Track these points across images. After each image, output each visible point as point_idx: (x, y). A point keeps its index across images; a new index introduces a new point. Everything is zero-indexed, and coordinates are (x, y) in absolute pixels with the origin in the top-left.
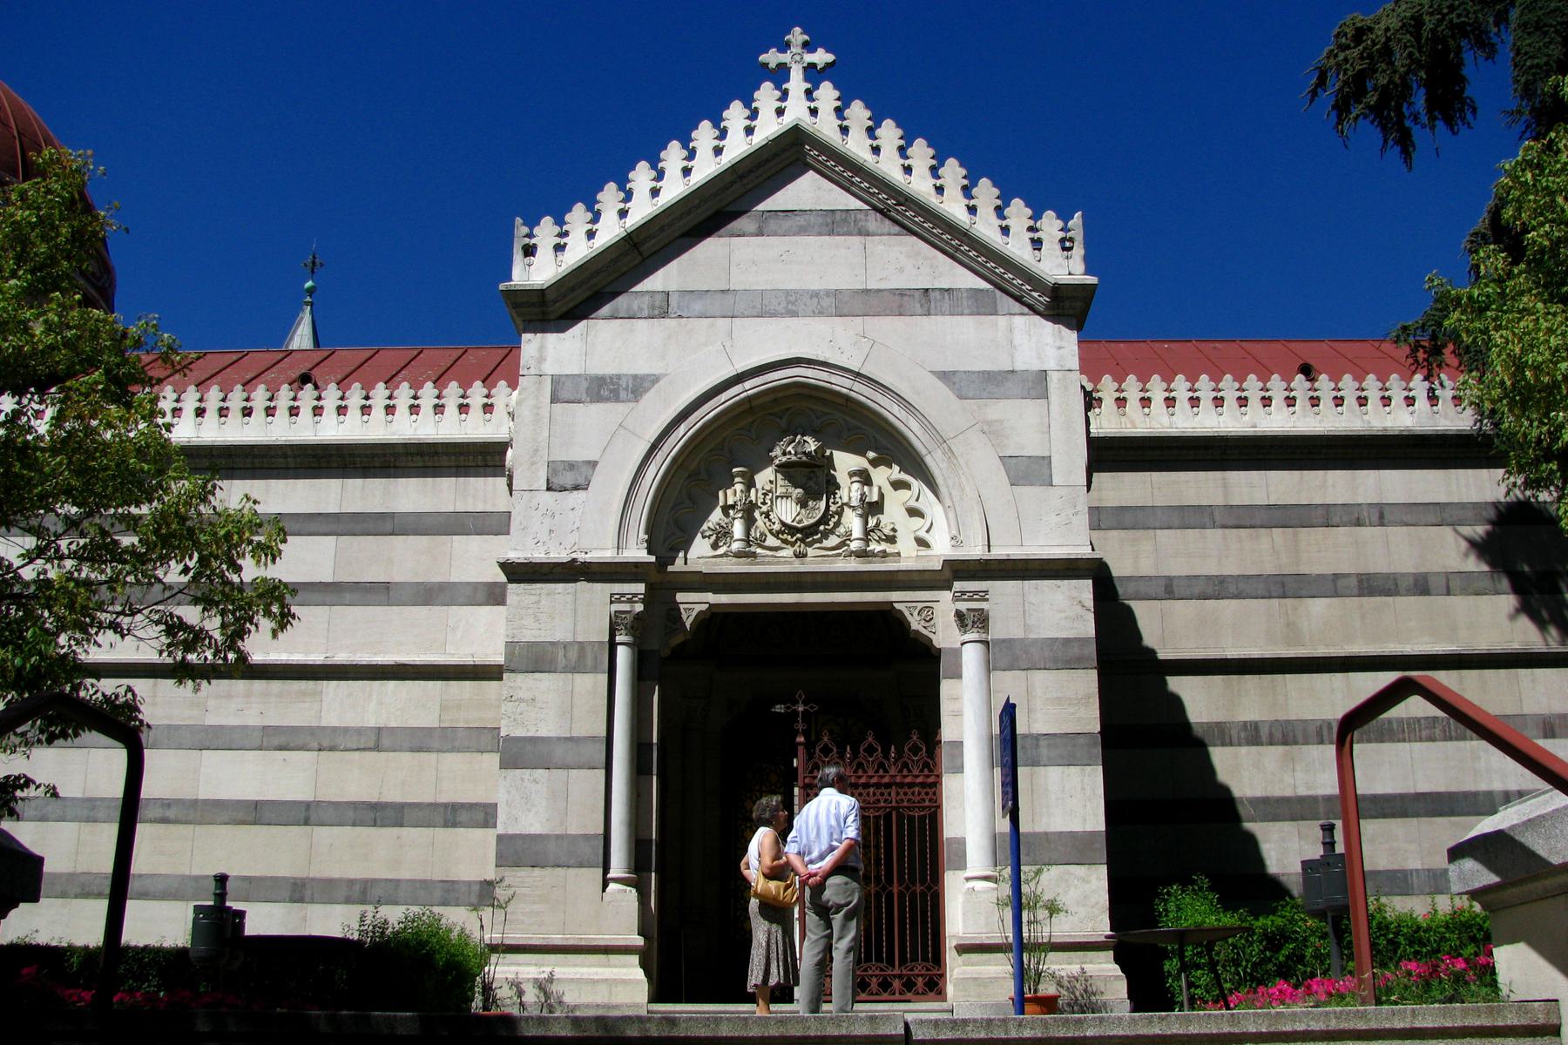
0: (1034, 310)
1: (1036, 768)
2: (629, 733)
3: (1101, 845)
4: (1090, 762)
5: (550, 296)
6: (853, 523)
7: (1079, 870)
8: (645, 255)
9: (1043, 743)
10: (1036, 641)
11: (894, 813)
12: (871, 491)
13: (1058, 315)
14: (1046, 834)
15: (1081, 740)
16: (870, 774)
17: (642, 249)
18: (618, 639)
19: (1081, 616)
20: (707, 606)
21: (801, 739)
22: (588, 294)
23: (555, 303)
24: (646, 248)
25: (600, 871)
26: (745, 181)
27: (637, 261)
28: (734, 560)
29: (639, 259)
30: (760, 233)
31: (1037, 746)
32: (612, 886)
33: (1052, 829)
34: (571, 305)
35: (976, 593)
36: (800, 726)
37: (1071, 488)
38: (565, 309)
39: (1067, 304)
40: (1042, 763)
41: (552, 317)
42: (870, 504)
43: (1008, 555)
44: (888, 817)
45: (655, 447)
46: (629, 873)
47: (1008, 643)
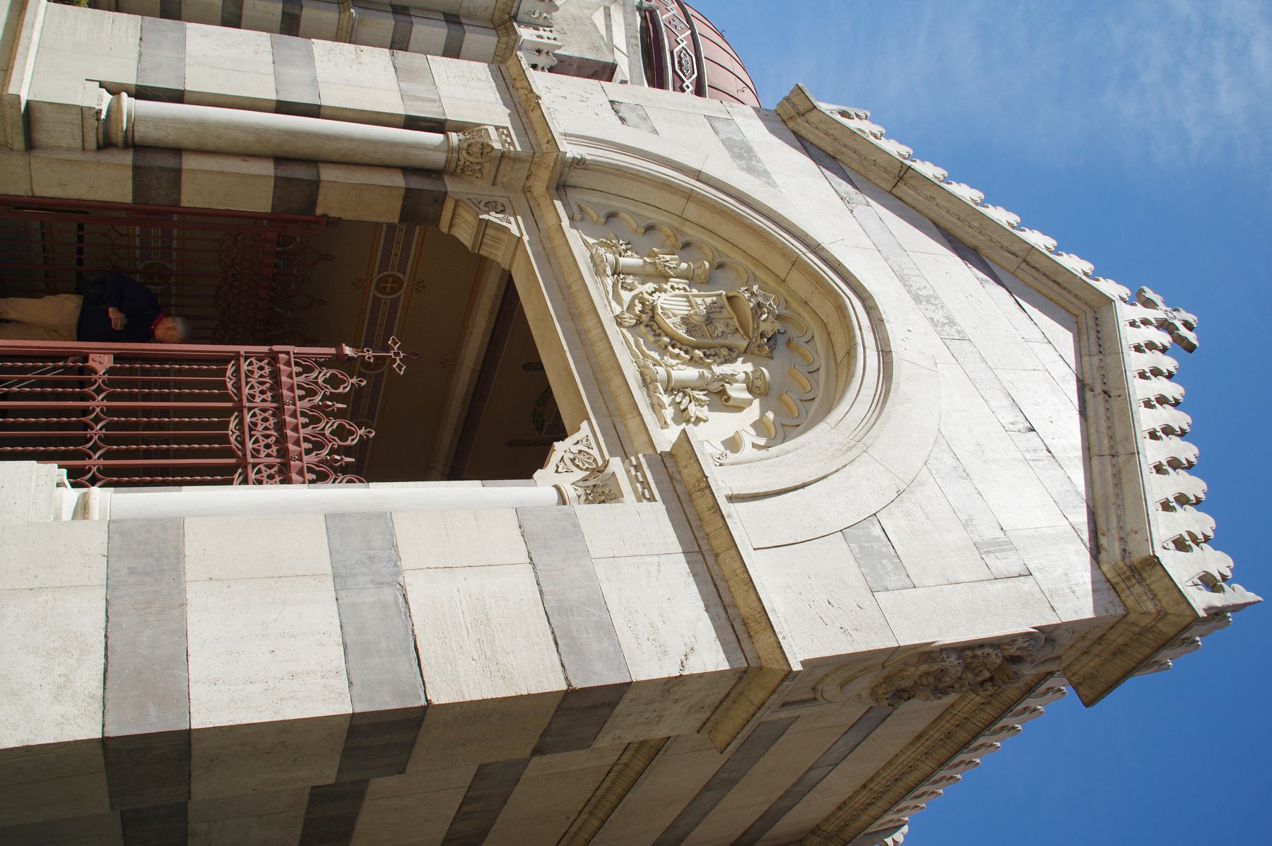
0: (1096, 551)
1: (330, 583)
2: (329, 132)
3: (154, 722)
4: (357, 687)
5: (812, 116)
6: (689, 373)
7: (90, 676)
8: (895, 191)
9: (388, 594)
10: (592, 576)
11: (233, 461)
12: (740, 390)
13: (1113, 587)
14: (183, 605)
15: (406, 666)
16: (305, 458)
17: (901, 186)
18: (454, 137)
19: (665, 654)
20: (518, 235)
21: (348, 351)
22: (830, 150)
23: (807, 122)
24: (902, 190)
25: (131, 79)
26: (1024, 266)
27: (884, 185)
28: (589, 254)
29: (888, 186)
30: (981, 281)
31: (380, 585)
32: (108, 97)
33: (192, 618)
34: (811, 137)
35: (645, 484)
36: (369, 354)
37: (883, 622)
38: (804, 133)
39: (1138, 589)
40: (342, 594)
41: (790, 126)
42: (722, 392)
43: (729, 516)
44: (230, 453)
45: (698, 175)
46: (129, 116)
47: (574, 530)
